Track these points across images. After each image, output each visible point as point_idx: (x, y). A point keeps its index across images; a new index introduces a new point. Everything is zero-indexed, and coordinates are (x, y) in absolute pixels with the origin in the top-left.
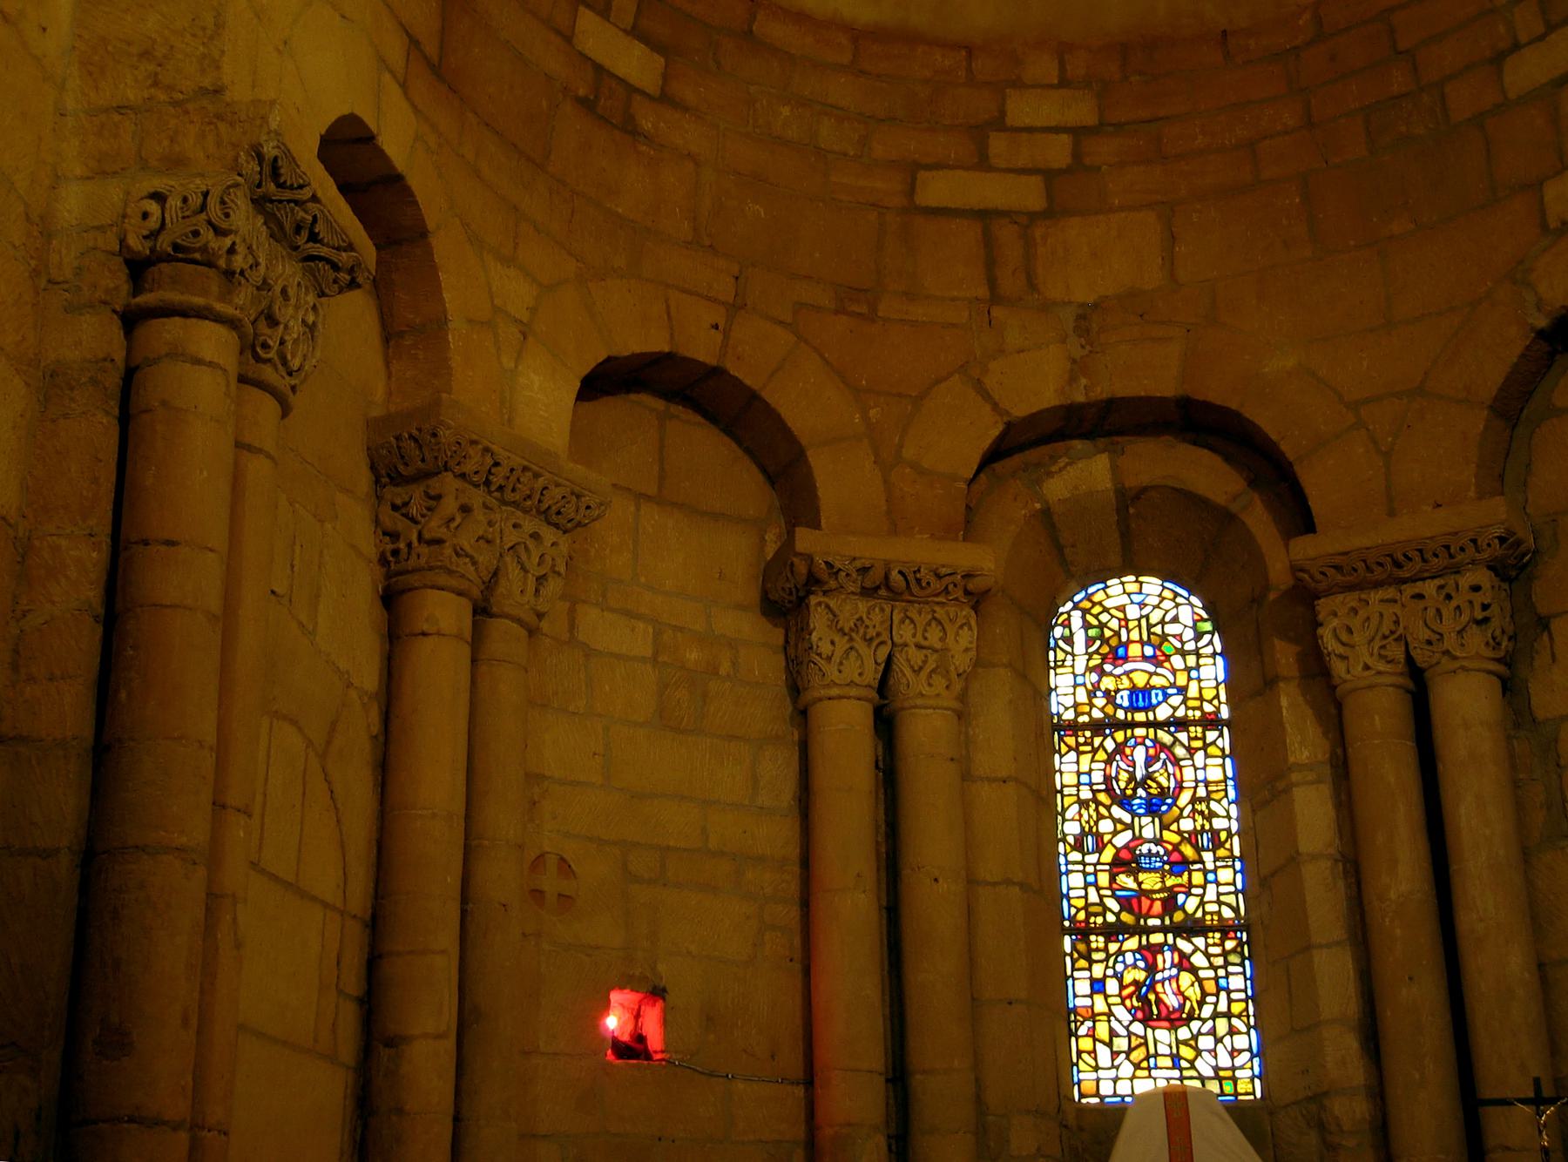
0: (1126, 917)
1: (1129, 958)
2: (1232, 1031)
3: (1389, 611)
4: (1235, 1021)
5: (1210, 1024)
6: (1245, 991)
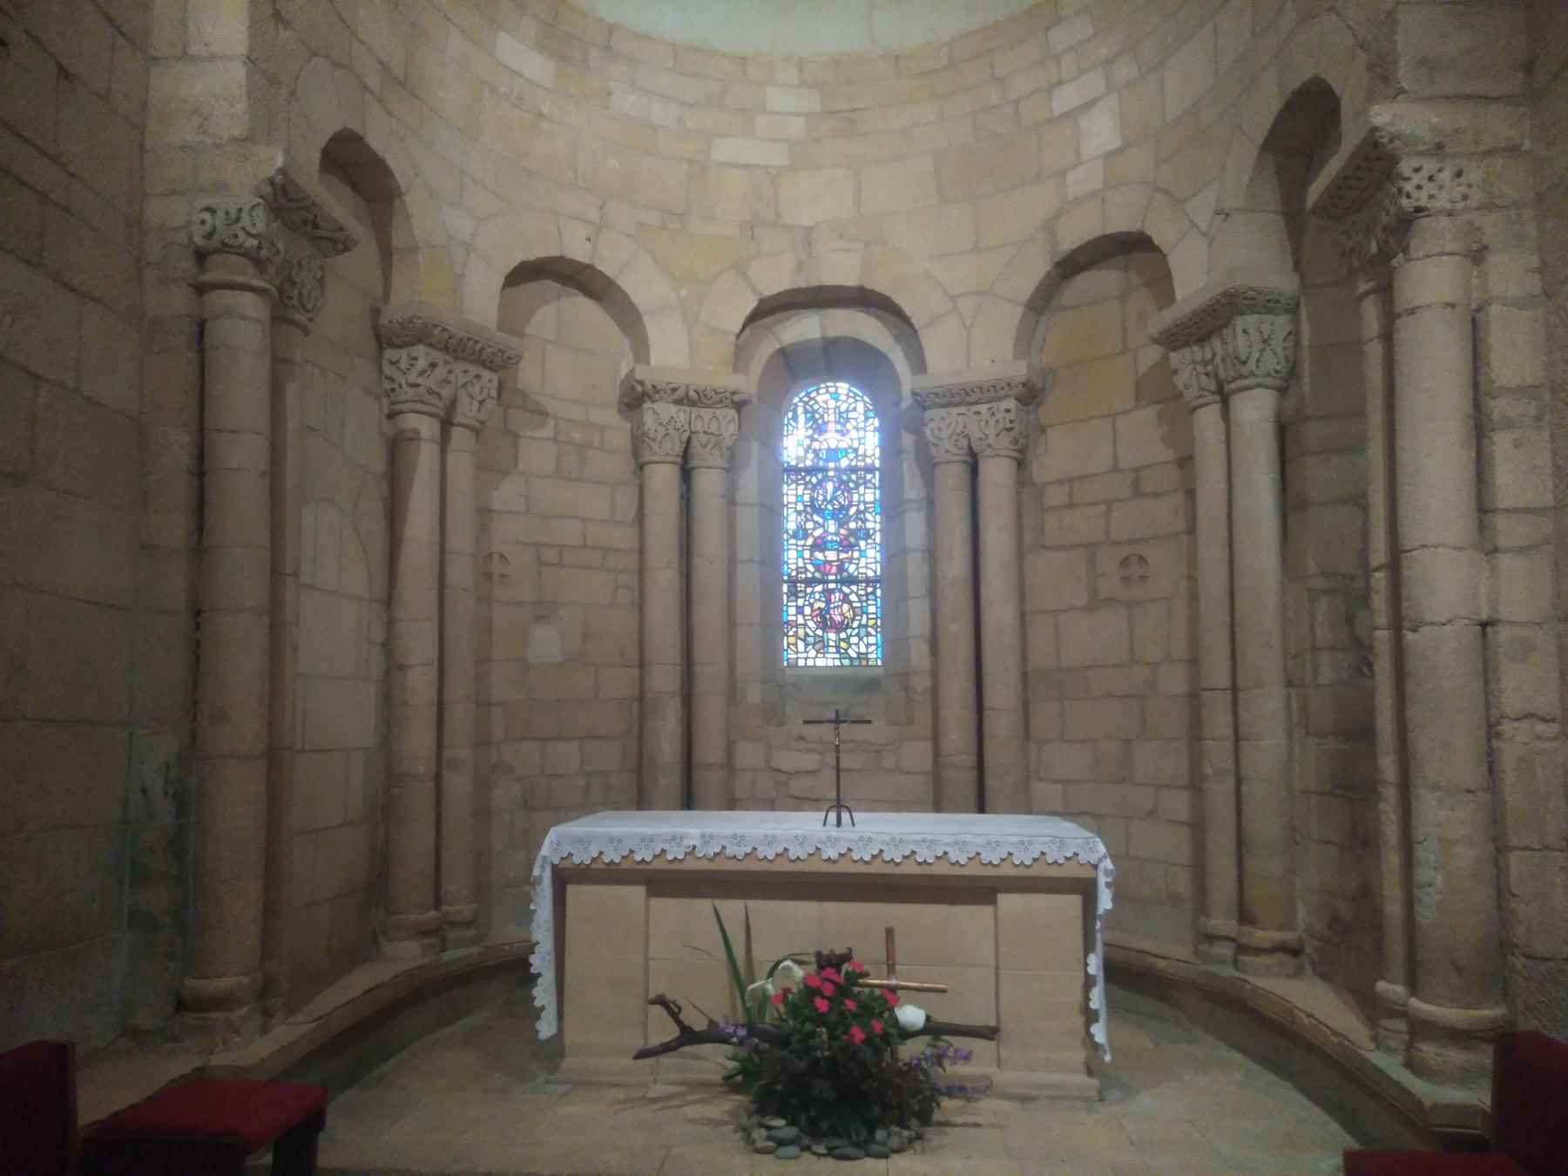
0: (817, 575)
1: (817, 596)
2: (868, 634)
3: (961, 419)
4: (870, 630)
5: (857, 631)
6: (876, 614)
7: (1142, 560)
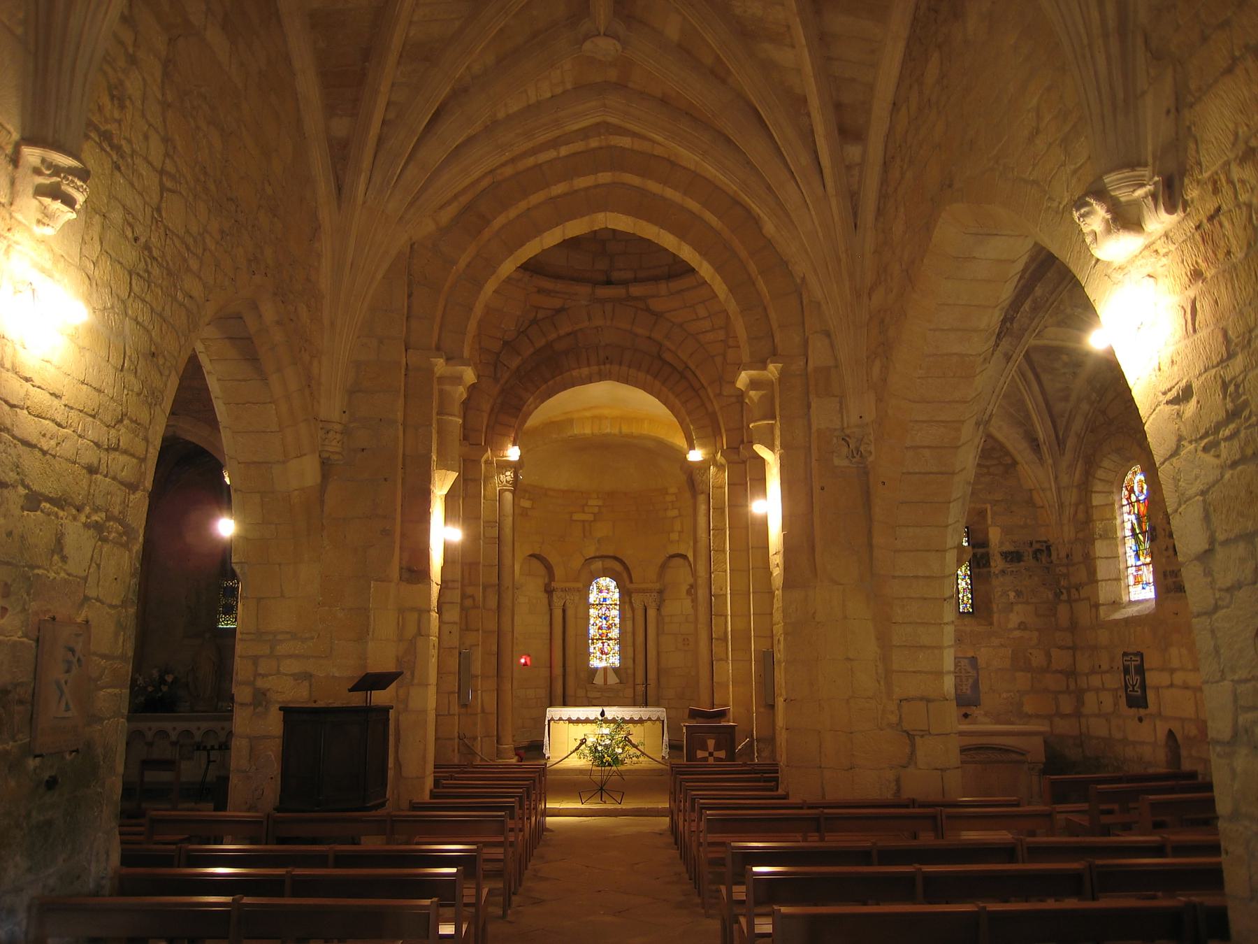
7: (688, 639)
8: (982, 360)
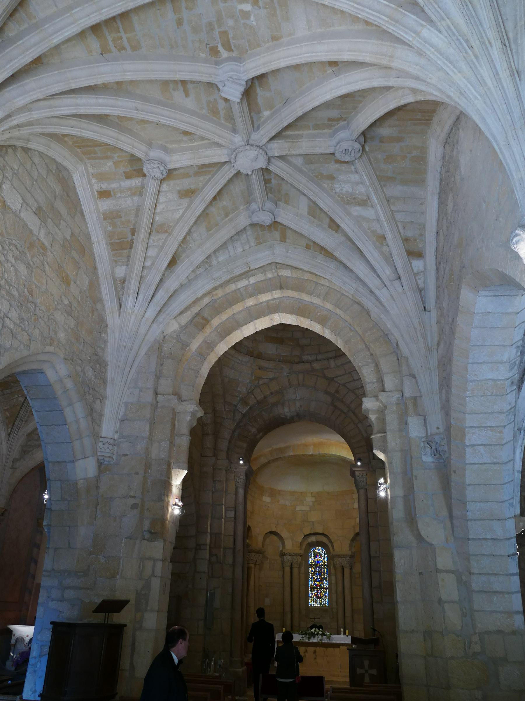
8: (510, 383)
